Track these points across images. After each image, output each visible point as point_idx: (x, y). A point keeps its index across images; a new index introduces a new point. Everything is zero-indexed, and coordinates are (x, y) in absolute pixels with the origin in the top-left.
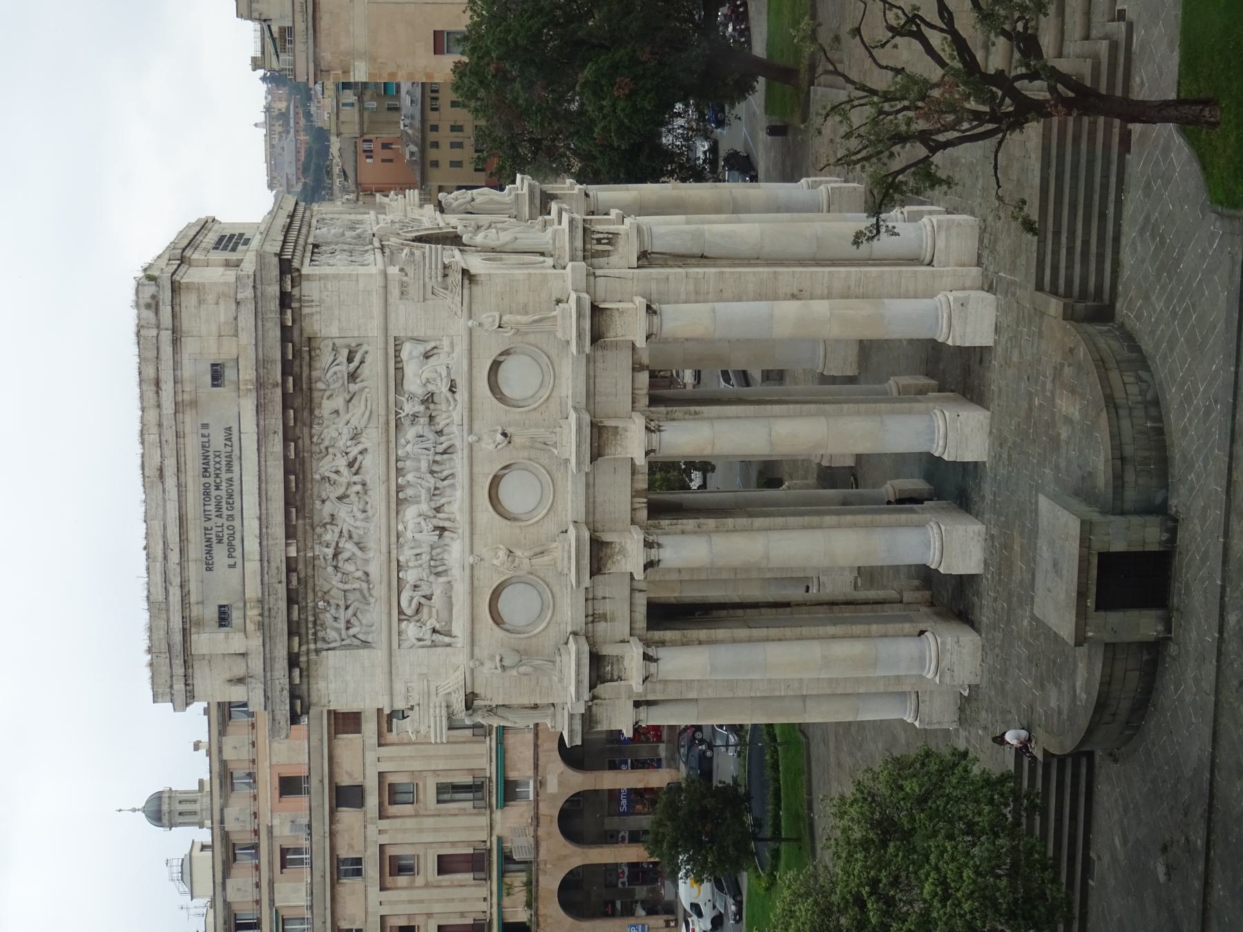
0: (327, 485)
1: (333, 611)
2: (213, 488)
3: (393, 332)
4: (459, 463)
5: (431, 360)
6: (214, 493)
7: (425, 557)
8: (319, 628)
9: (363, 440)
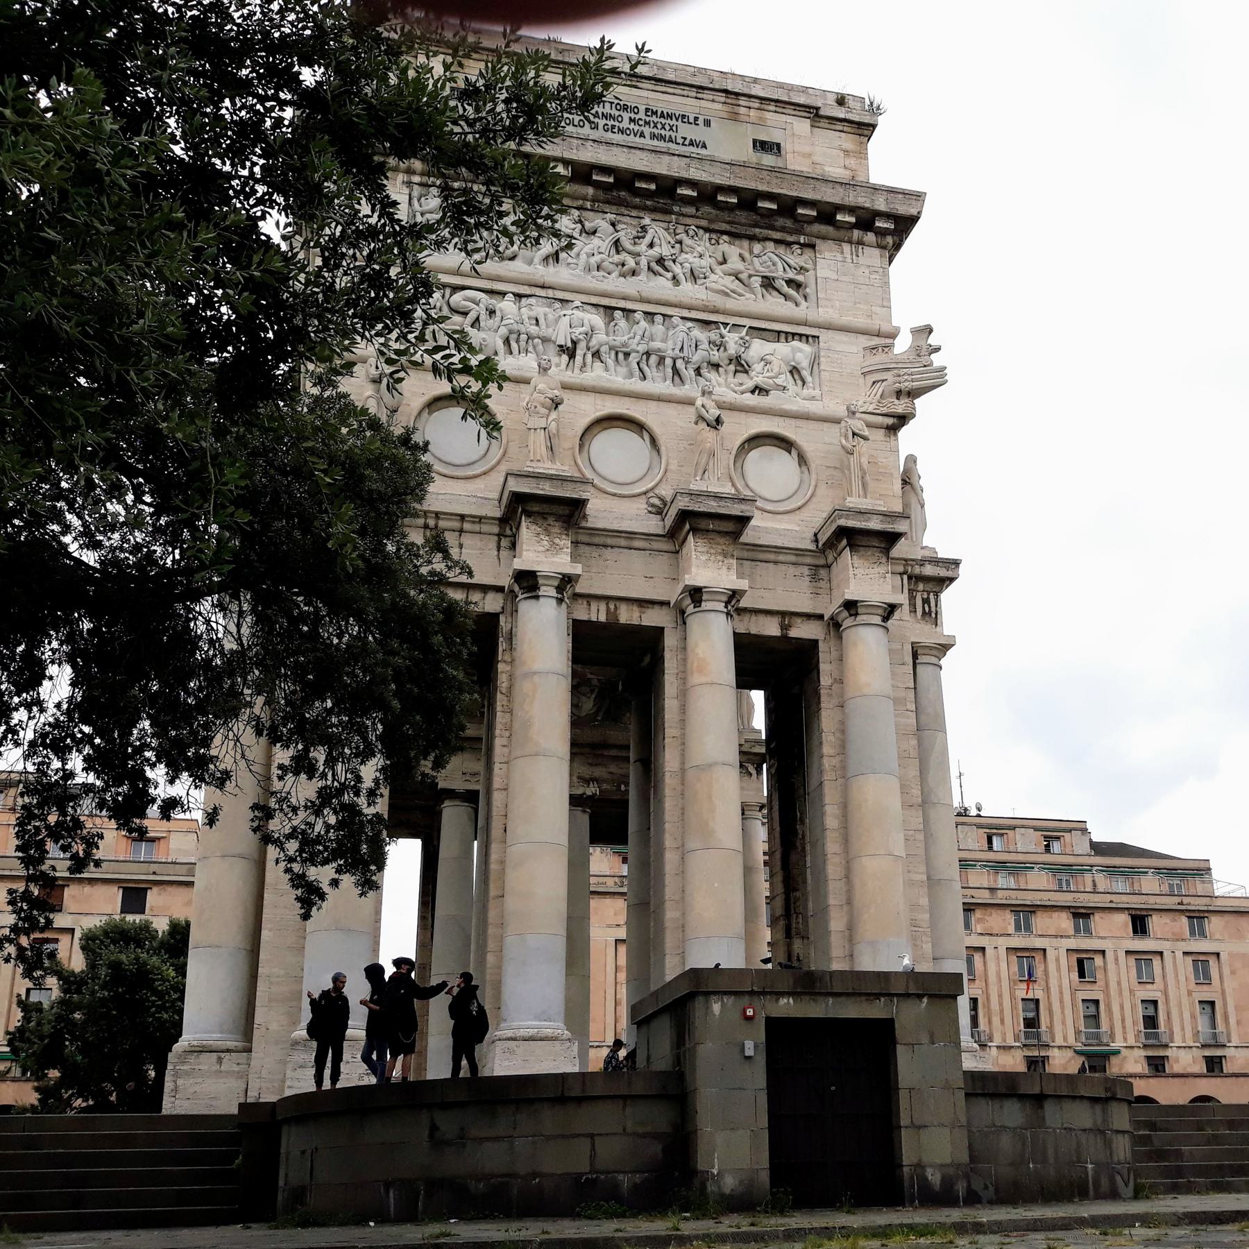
0: (635, 233)
2: (633, 116)
3: (824, 336)
4: (659, 384)
6: (626, 116)
7: (533, 330)
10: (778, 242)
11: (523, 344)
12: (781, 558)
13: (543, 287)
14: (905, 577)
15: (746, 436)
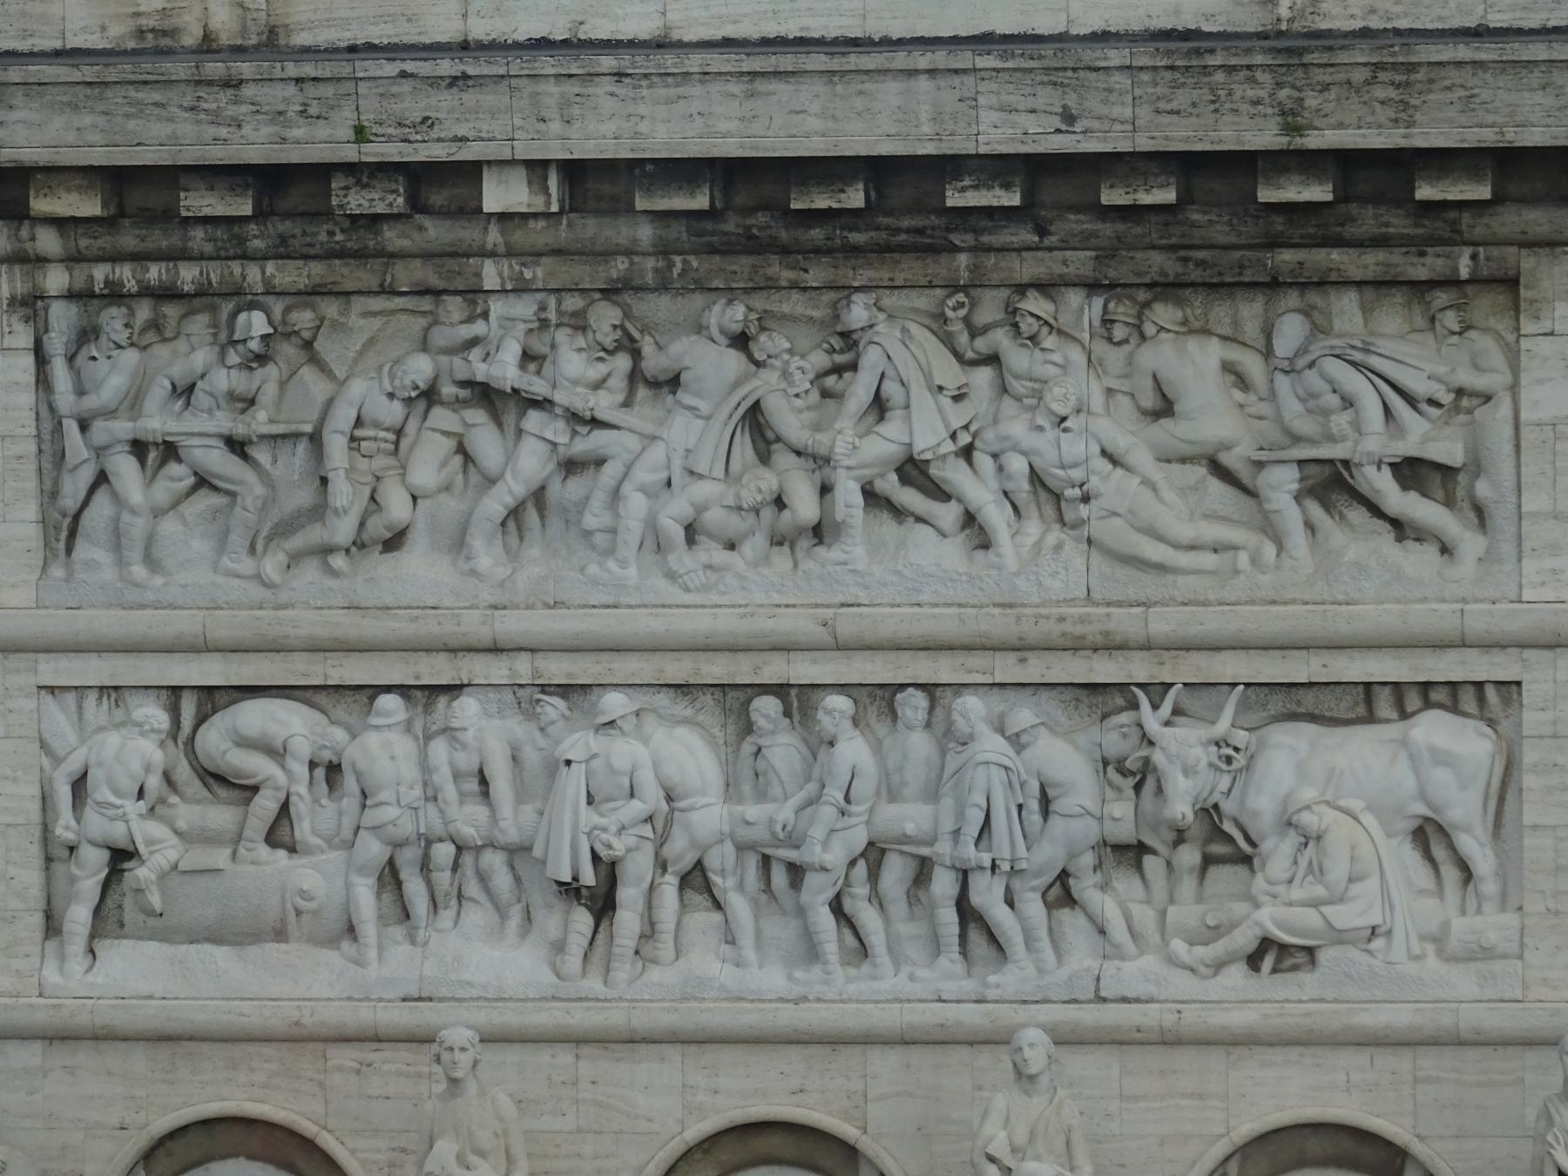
0: (819, 360)
1: (222, 380)
3: (1540, 677)
4: (913, 979)
5: (1411, 855)
7: (469, 820)
8: (144, 312)
9: (1033, 528)
11: (443, 878)
13: (495, 649)
15: (1248, 1127)
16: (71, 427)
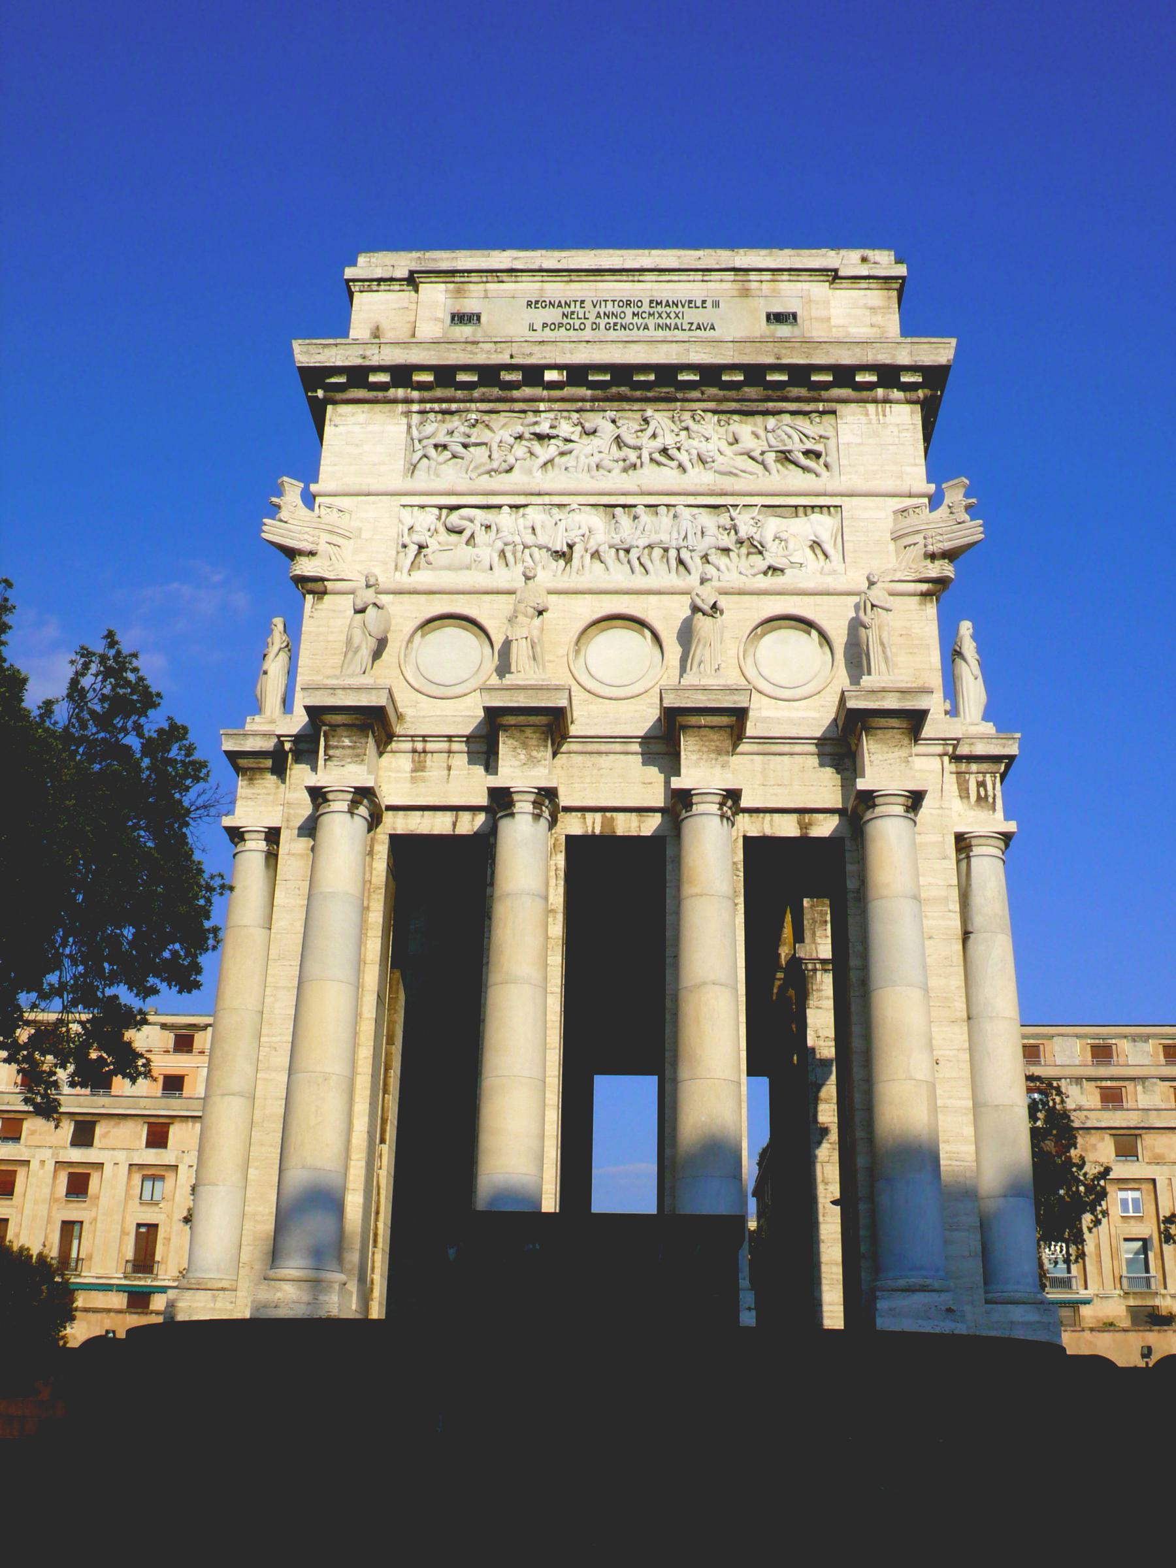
1: (463, 429)
2: (636, 310)
5: (809, 551)
6: (629, 311)
7: (529, 539)
8: (440, 416)
10: (793, 413)
11: (519, 554)
12: (798, 748)
13: (539, 494)
14: (946, 759)
16: (416, 442)
